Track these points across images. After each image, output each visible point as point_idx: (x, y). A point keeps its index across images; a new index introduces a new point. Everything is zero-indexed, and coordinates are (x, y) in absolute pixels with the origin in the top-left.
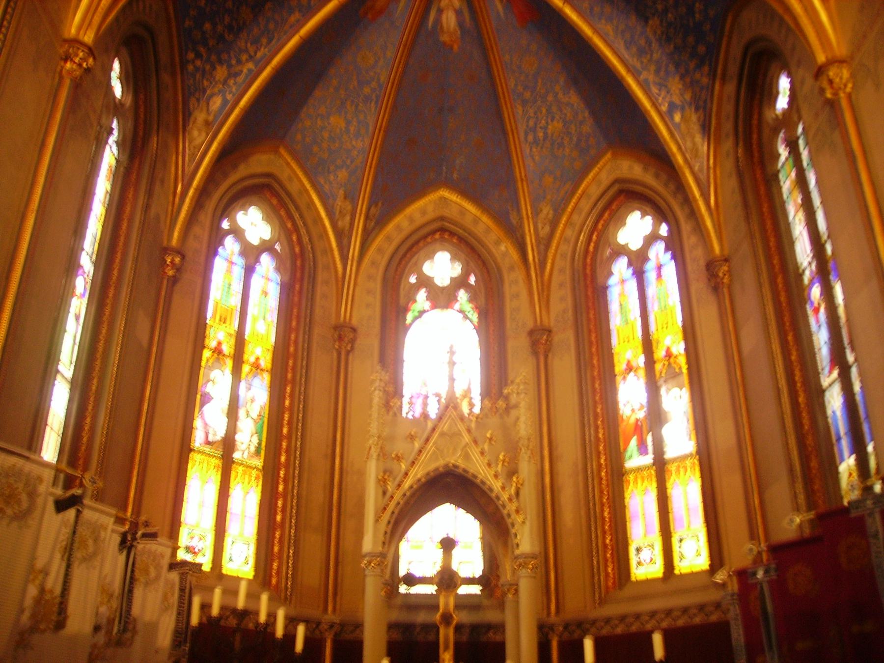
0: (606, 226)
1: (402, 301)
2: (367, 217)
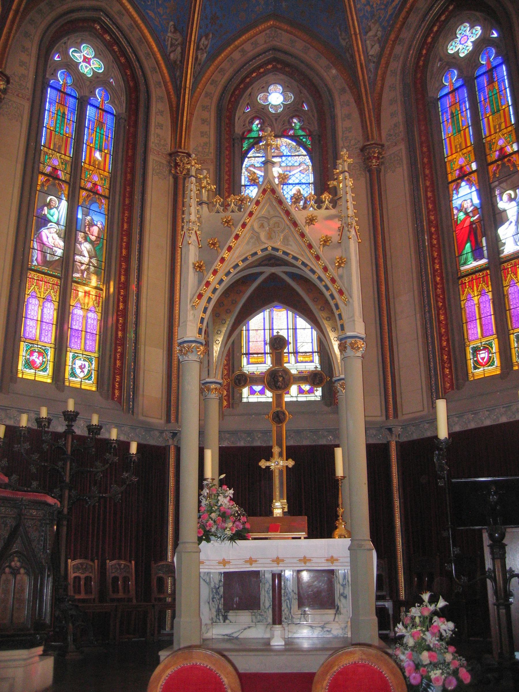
0: (435, 40)
1: (238, 130)
2: (198, 48)
